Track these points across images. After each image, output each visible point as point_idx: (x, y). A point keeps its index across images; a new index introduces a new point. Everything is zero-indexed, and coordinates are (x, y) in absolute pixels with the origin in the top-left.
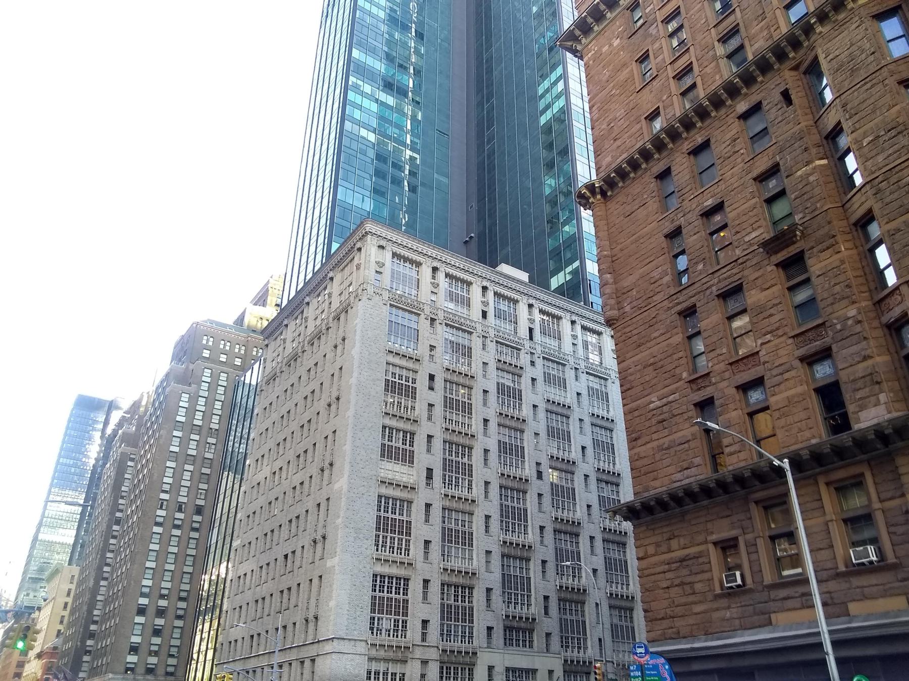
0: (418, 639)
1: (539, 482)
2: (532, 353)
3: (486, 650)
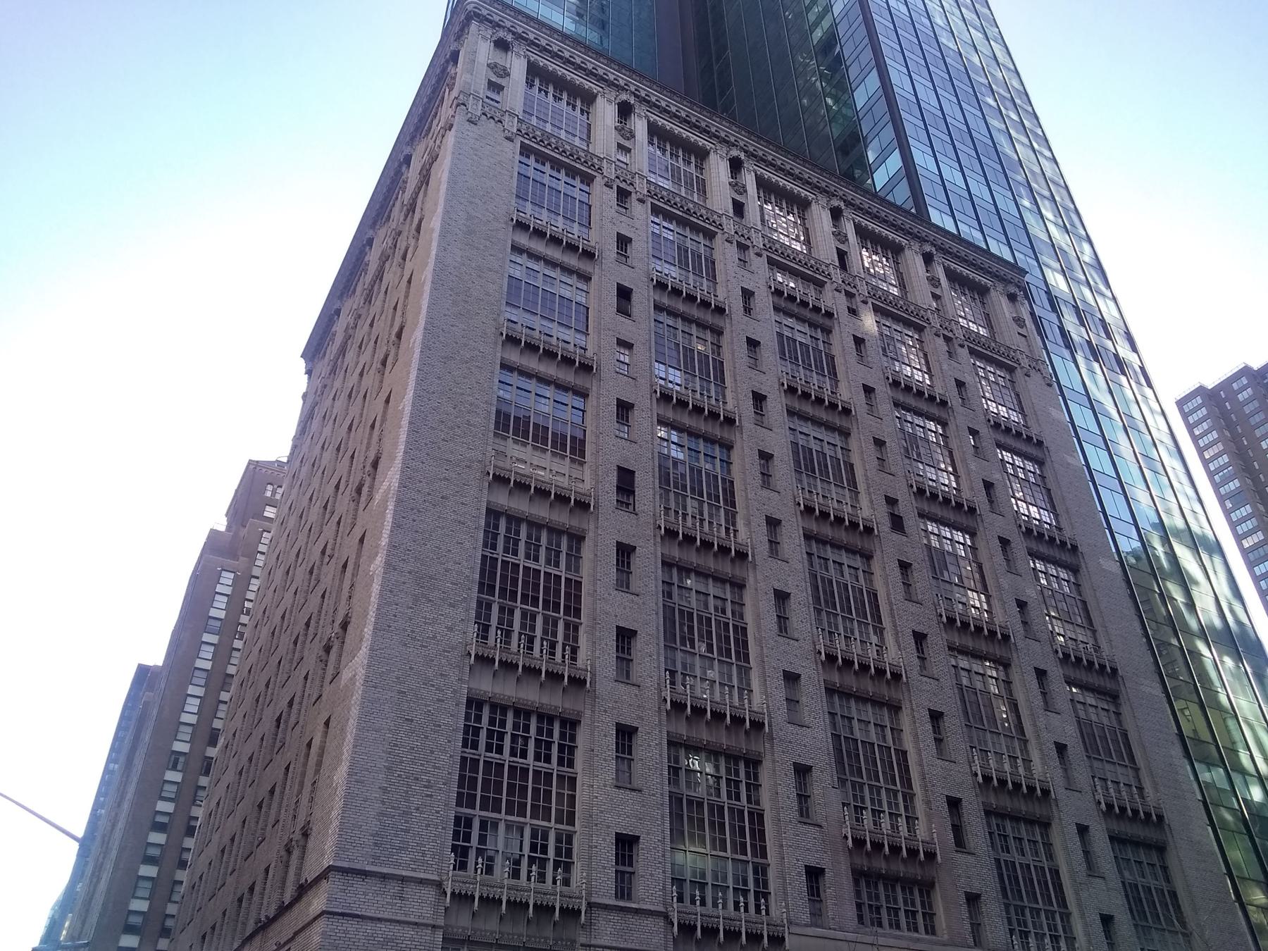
1: (896, 537)
2: (849, 295)
3: (810, 931)
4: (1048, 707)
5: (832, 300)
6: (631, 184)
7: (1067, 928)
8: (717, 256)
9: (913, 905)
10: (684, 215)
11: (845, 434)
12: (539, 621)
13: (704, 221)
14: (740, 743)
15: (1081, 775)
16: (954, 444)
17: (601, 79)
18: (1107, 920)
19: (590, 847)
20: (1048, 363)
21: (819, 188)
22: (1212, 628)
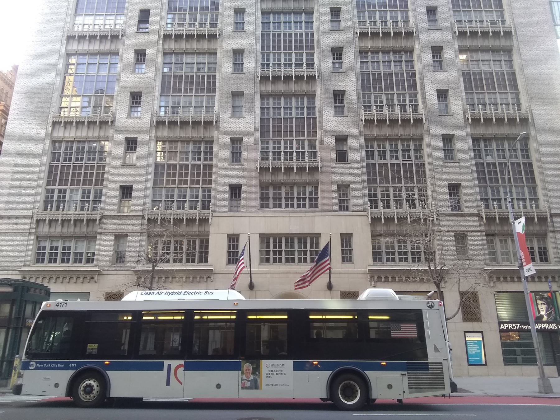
14: (200, 133)
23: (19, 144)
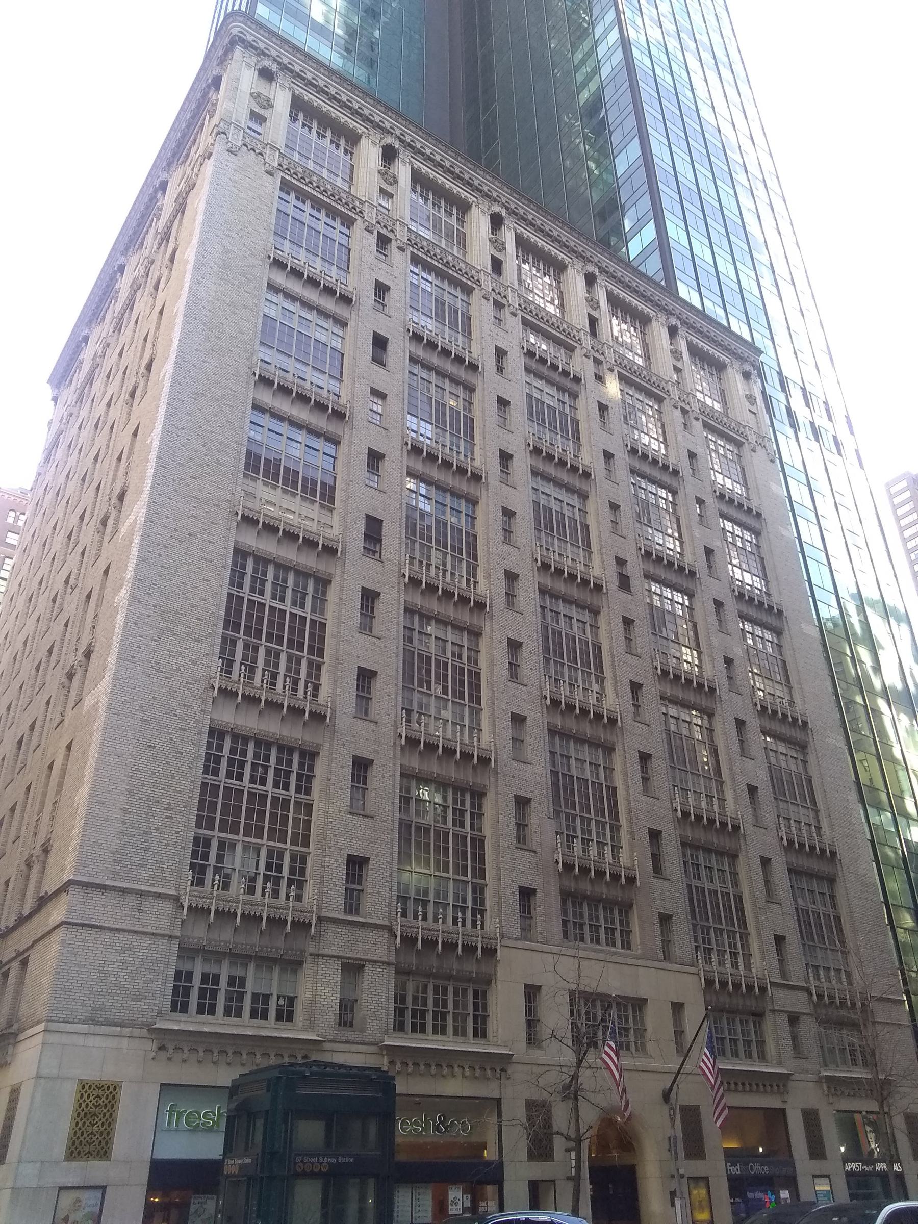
0: (335, 907)
1: (622, 595)
2: (597, 362)
3: (520, 944)
4: (744, 753)
5: (581, 365)
6: (392, 231)
7: (745, 945)
8: (474, 312)
9: (613, 923)
10: (443, 268)
11: (584, 496)
12: (283, 658)
13: (463, 276)
14: (467, 776)
15: (768, 814)
16: (681, 512)
17: (366, 119)
18: (779, 940)
19: (323, 867)
20: (773, 440)
21: (575, 252)
22: (894, 689)
23: (145, 720)
